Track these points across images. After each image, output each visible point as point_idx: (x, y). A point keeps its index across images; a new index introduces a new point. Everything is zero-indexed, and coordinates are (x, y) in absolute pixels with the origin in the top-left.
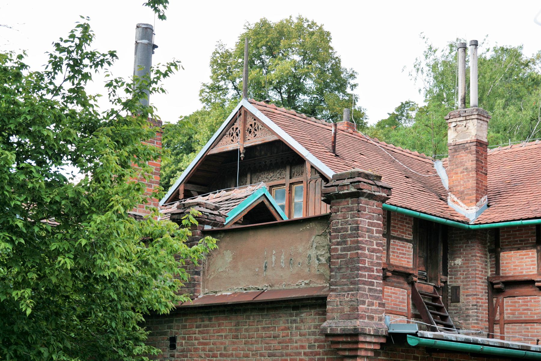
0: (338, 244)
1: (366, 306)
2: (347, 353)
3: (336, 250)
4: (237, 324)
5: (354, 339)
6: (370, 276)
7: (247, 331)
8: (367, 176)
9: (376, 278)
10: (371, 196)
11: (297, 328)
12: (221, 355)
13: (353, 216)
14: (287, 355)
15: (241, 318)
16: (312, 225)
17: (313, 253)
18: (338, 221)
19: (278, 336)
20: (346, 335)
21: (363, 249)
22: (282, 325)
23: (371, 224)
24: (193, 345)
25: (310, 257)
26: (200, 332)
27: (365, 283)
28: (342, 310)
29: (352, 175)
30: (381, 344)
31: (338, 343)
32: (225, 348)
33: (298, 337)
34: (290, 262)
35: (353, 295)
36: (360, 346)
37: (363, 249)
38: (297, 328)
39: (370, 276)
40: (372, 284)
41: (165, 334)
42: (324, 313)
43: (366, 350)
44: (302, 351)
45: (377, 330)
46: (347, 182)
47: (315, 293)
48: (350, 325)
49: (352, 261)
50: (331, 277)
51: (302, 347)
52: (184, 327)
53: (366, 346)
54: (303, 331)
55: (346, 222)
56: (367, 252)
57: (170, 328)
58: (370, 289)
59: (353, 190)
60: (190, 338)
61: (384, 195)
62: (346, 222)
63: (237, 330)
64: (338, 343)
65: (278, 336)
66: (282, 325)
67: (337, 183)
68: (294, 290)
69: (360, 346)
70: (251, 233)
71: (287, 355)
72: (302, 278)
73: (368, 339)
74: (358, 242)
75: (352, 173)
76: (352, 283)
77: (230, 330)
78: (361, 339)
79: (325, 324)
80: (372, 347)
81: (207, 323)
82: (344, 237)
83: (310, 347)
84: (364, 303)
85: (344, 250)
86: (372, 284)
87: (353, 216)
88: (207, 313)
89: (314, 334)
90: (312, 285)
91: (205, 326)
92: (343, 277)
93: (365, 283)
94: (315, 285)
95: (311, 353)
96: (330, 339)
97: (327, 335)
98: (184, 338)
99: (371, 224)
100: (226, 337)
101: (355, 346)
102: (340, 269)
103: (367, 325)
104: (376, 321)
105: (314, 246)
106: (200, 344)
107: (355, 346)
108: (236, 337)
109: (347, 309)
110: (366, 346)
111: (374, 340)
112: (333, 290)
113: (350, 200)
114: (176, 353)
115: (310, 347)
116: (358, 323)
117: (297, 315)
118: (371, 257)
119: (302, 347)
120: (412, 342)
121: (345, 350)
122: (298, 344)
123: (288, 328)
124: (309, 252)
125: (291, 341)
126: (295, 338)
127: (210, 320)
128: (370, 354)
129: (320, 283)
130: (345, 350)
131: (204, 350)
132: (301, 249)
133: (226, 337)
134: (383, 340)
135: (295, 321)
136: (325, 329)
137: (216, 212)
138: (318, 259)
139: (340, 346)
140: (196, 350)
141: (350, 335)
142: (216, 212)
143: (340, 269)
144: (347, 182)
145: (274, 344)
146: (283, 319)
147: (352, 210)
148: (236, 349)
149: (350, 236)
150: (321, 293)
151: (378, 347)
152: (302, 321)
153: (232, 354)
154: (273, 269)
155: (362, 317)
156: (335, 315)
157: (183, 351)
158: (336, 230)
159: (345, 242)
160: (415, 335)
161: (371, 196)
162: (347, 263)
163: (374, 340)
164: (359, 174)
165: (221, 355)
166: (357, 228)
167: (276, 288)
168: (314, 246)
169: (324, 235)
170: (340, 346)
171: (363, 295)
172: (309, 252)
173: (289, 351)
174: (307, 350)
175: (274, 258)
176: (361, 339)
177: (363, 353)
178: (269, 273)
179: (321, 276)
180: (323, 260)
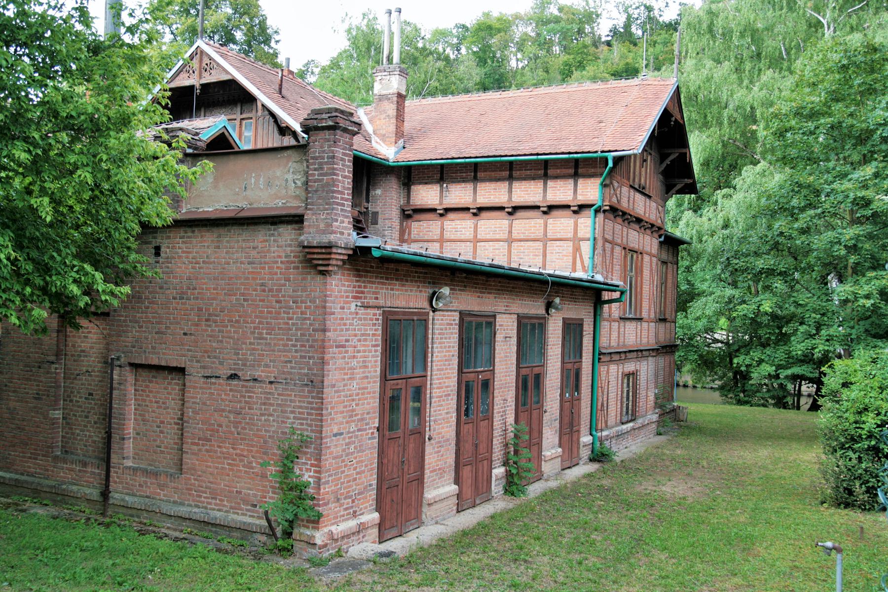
0: (315, 170)
1: (338, 224)
2: (321, 262)
3: (313, 175)
4: (219, 236)
5: (328, 250)
6: (342, 199)
7: (228, 242)
8: (342, 112)
9: (347, 200)
10: (345, 130)
11: (274, 241)
12: (204, 262)
13: (330, 146)
14: (265, 263)
15: (222, 231)
16: (289, 152)
17: (290, 177)
18: (315, 149)
19: (257, 247)
20: (321, 247)
21: (337, 175)
22: (261, 238)
23: (344, 154)
24: (177, 253)
25: (287, 180)
26: (183, 242)
27: (338, 204)
28: (318, 226)
29: (329, 111)
30: (349, 255)
31: (314, 253)
32: (207, 257)
33: (276, 248)
34: (269, 184)
35: (328, 214)
36: (333, 256)
37: (337, 175)
38: (274, 241)
39: (342, 199)
40: (343, 205)
41: (150, 243)
42: (301, 228)
43: (337, 259)
44: (279, 260)
45: (346, 244)
46: (325, 116)
47: (293, 212)
48: (325, 239)
49: (328, 184)
50: (307, 199)
51: (280, 257)
52: (169, 237)
53: (337, 257)
54: (280, 243)
55: (324, 152)
56: (340, 178)
57: (155, 238)
58: (342, 210)
59: (331, 123)
60: (174, 247)
61: (356, 129)
62: (324, 152)
63: (219, 241)
64: (314, 253)
65: (257, 247)
66: (261, 238)
67: (316, 116)
68: (272, 208)
69: (333, 256)
70: (232, 157)
71: (265, 263)
72: (279, 198)
73: (339, 251)
74: (334, 169)
75: (329, 109)
76: (327, 204)
77: (212, 241)
78: (334, 250)
79: (302, 238)
80: (342, 257)
81: (190, 234)
82: (321, 164)
83: (286, 257)
84: (337, 221)
85: (319, 175)
86: (343, 205)
87: (330, 146)
88: (191, 226)
89: (290, 245)
90: (288, 205)
91: (189, 237)
92: (320, 198)
93: (338, 204)
94: (292, 205)
95: (288, 262)
96: (307, 250)
97: (304, 247)
98: (168, 247)
99: (344, 154)
100: (208, 247)
101: (328, 256)
102: (316, 191)
103: (339, 239)
104: (346, 236)
105: (291, 170)
106: (183, 252)
107: (328, 256)
108: (218, 247)
109: (322, 226)
110: (337, 257)
111: (344, 251)
112: (310, 209)
113: (327, 132)
114: (161, 260)
115: (286, 257)
116: (332, 238)
117: (274, 230)
118: (343, 182)
119: (280, 257)
120: (376, 253)
121: (319, 259)
122: (276, 254)
123: (267, 241)
124: (286, 176)
125: (269, 251)
126: (272, 249)
127: (193, 232)
128: (340, 263)
129: (295, 203)
130: (319, 259)
131: (187, 257)
132: (278, 173)
133: (208, 247)
134: (351, 252)
135: (273, 235)
136: (303, 242)
137: (196, 138)
138: (295, 183)
139: (315, 256)
140: (180, 257)
141: (325, 247)
142: (196, 138)
143: (316, 191)
144: (325, 116)
145: (254, 253)
146: (262, 233)
147: (329, 140)
148: (218, 258)
149: (326, 163)
150: (299, 211)
151: (346, 257)
152: (279, 235)
153: (214, 262)
154: (252, 190)
155: (335, 233)
156: (311, 230)
157: (167, 258)
158: (313, 158)
159: (322, 169)
160: (379, 248)
161: (345, 130)
162: (323, 186)
163: (344, 251)
164: (336, 110)
165: (204, 262)
166: (334, 157)
167: (255, 206)
168: (291, 170)
169: (301, 161)
170: (315, 256)
171: (336, 214)
172: (286, 176)
173: (267, 260)
174: (284, 259)
175: (253, 180)
176: (334, 250)
177: (334, 262)
178: (248, 193)
179: (297, 197)
180: (299, 183)
